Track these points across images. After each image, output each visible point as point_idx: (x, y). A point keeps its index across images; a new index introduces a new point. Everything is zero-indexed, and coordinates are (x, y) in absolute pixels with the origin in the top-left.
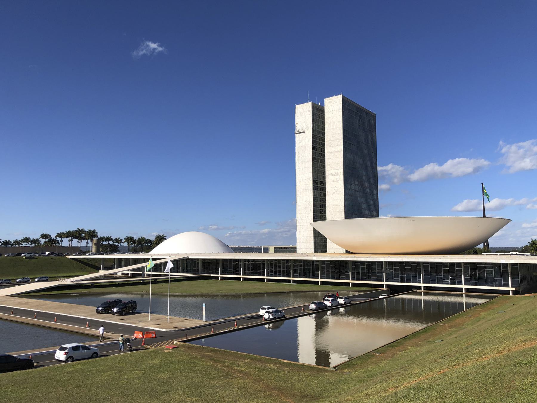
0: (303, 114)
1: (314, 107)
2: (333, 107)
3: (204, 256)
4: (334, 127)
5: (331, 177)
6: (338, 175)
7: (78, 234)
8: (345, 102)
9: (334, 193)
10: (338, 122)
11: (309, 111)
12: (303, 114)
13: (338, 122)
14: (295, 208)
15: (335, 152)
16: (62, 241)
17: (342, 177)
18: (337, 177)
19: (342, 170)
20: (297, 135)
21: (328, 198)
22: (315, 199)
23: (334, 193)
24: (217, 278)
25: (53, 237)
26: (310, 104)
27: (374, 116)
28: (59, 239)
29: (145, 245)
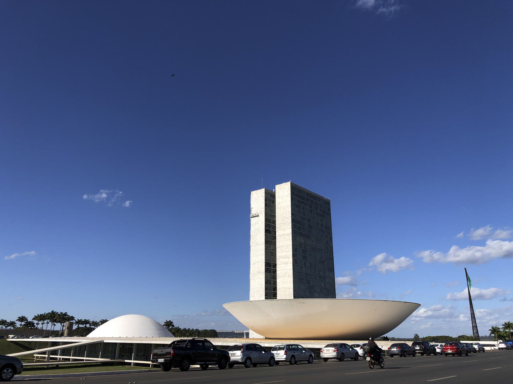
0: (257, 199)
1: (266, 193)
2: (283, 193)
3: (124, 340)
4: (284, 211)
5: (281, 260)
6: (288, 257)
7: (53, 317)
8: (293, 189)
9: (284, 276)
10: (288, 207)
11: (262, 196)
12: (257, 199)
13: (288, 207)
14: (249, 290)
15: (284, 235)
16: (37, 324)
17: (291, 260)
18: (287, 260)
19: (291, 253)
20: (252, 219)
21: (278, 280)
22: (267, 282)
23: (284, 276)
24: (130, 364)
25: (30, 319)
26: (263, 191)
27: (327, 203)
28: (35, 322)
29: (86, 327)
